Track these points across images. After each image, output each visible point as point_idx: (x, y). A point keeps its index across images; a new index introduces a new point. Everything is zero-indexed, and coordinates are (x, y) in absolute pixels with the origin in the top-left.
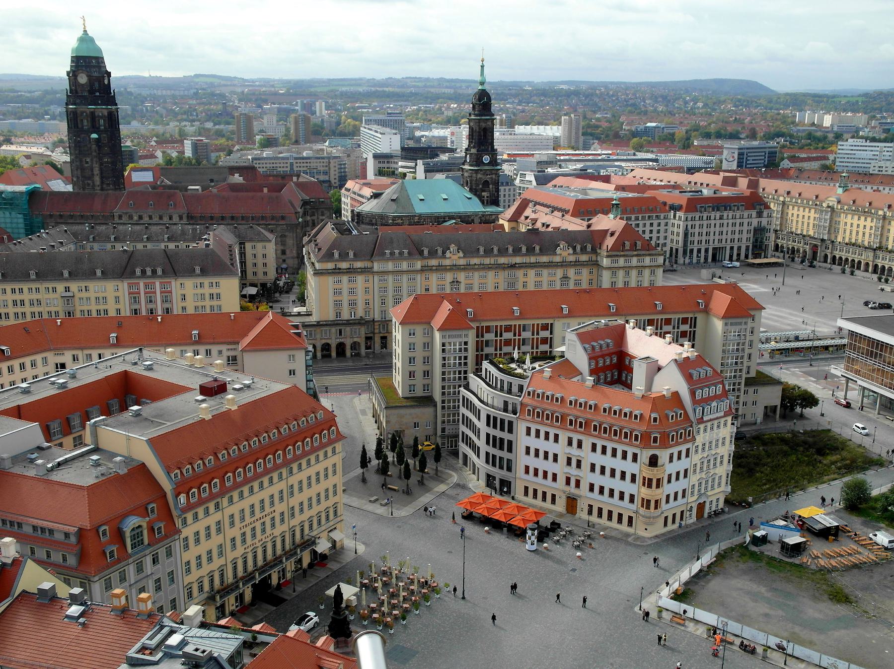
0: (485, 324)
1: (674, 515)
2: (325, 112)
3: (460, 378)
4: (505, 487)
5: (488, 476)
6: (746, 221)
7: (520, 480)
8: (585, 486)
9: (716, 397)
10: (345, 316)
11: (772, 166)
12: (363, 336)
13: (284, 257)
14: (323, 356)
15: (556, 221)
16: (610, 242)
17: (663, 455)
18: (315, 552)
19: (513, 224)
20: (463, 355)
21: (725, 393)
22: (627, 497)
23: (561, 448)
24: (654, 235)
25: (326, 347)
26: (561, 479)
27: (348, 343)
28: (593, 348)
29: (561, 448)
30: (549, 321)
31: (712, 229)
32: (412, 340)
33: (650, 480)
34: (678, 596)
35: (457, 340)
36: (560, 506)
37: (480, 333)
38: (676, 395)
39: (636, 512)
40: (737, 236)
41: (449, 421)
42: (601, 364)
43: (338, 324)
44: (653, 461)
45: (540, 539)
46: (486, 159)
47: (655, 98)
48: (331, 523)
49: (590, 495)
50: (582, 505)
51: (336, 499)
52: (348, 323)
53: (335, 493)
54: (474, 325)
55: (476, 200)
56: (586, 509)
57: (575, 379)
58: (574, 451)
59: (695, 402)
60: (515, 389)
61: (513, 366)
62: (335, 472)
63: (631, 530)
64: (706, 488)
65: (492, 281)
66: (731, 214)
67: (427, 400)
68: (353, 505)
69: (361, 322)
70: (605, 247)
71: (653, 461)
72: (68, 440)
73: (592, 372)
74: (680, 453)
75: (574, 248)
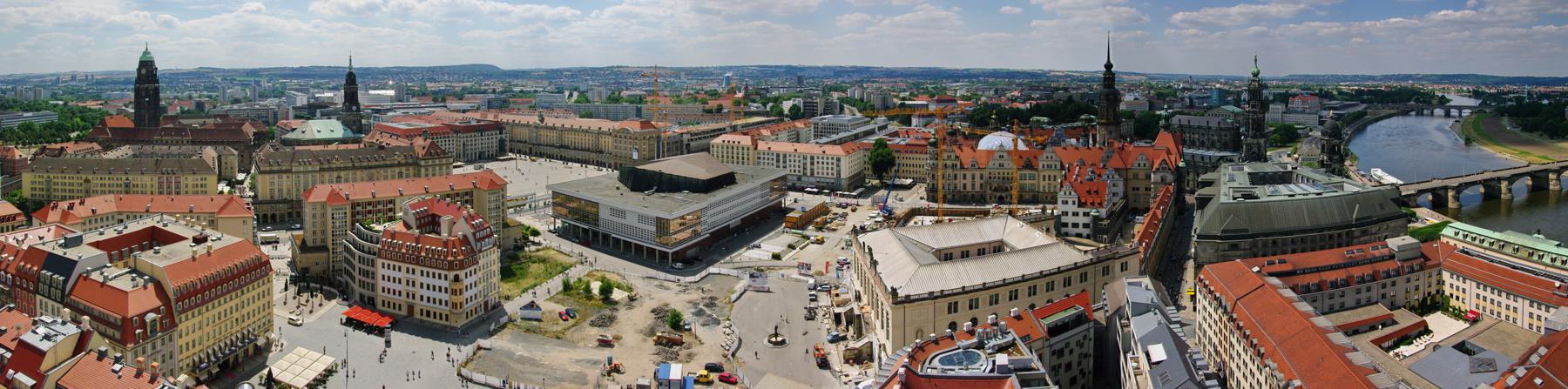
10: (276, 197)
17: (462, 274)
23: (402, 275)
25: (265, 216)
29: (402, 275)
43: (272, 202)
44: (457, 279)
50: (417, 310)
52: (279, 202)
58: (410, 276)
59: (477, 240)
67: (324, 248)
69: (285, 201)
71: (457, 279)
72: (121, 264)
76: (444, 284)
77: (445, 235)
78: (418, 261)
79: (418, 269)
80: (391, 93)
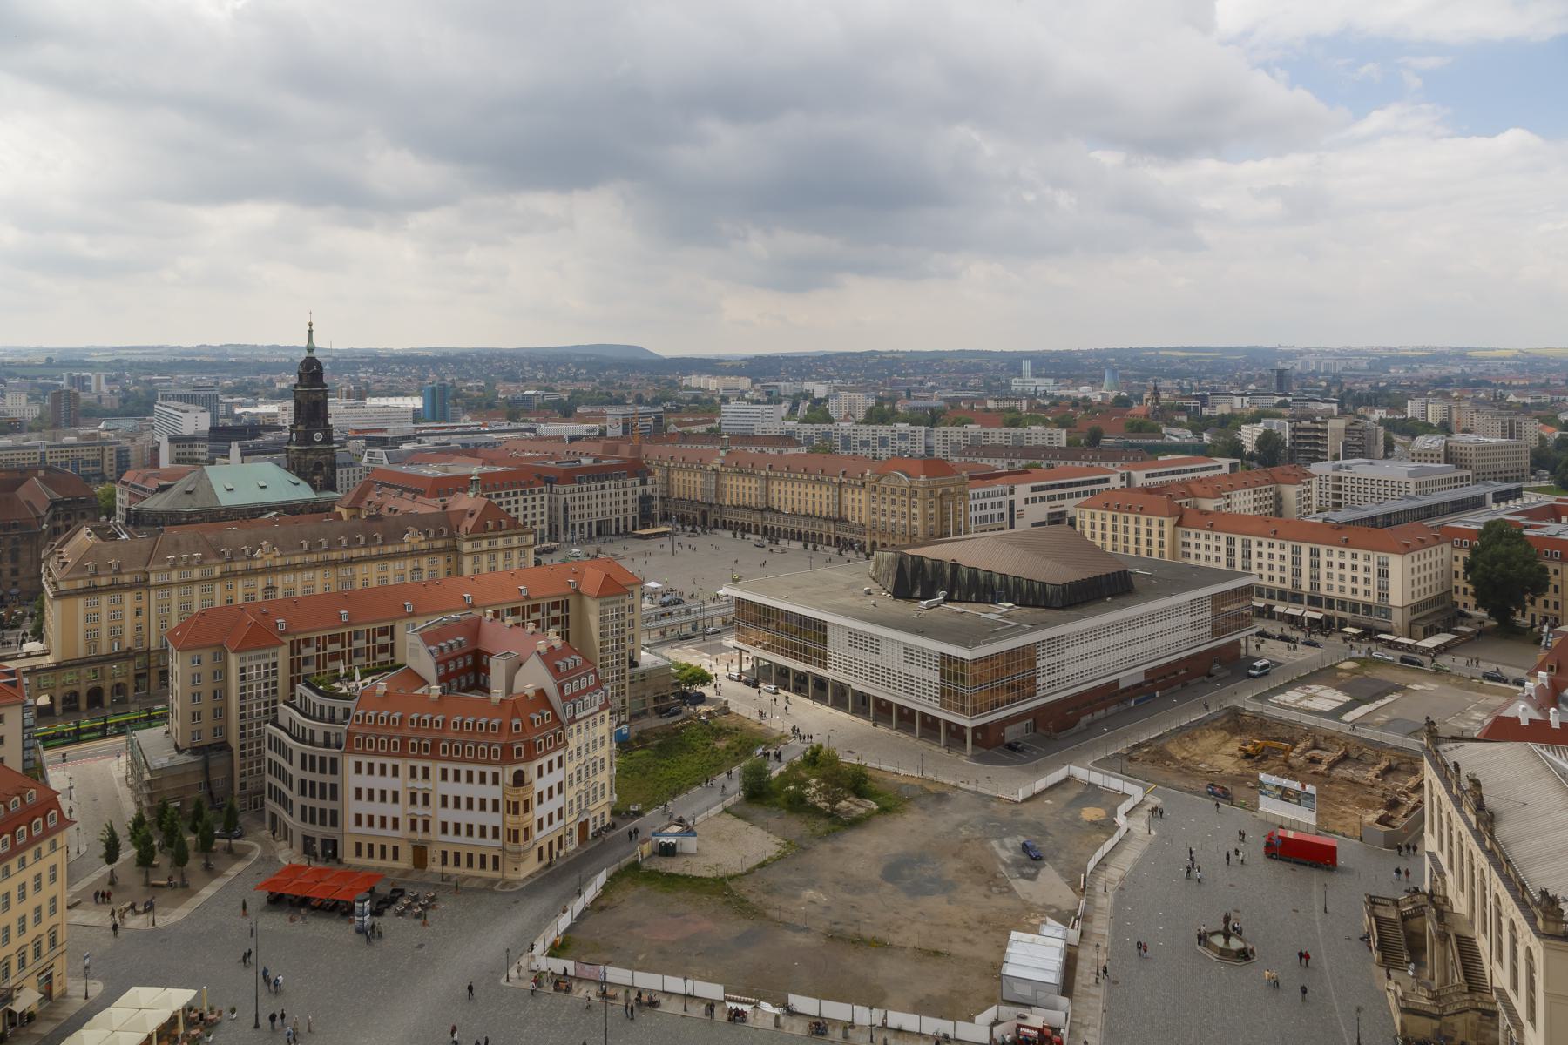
0: (301, 637)
1: (551, 844)
2: (105, 389)
3: (266, 712)
4: (331, 849)
5: (305, 838)
6: (630, 490)
7: (350, 833)
8: (435, 827)
9: (589, 689)
10: (104, 649)
11: (658, 431)
12: (132, 673)
13: (15, 579)
14: (65, 710)
15: (407, 505)
16: (469, 523)
17: (530, 770)
18: (11, 1013)
19: (353, 512)
20: (271, 680)
21: (599, 684)
22: (489, 832)
23: (402, 784)
24: (521, 513)
26: (404, 824)
27: (107, 685)
28: (441, 649)
29: (402, 784)
30: (389, 624)
31: (594, 501)
32: (197, 669)
33: (516, 804)
34: (556, 951)
35: (262, 662)
36: (405, 862)
37: (295, 648)
38: (541, 693)
39: (503, 849)
40: (621, 506)
41: (251, 772)
42: (452, 668)
43: (94, 661)
44: (519, 779)
45: (376, 913)
46: (318, 436)
47: (533, 365)
48: (45, 959)
49: (443, 838)
50: (434, 853)
51: (56, 919)
52: (109, 659)
53: (53, 910)
54: (287, 640)
55: (304, 485)
56: (439, 859)
57: (419, 692)
58: (419, 784)
59: (564, 698)
60: (339, 715)
61: (337, 685)
62: (53, 878)
63: (497, 875)
64: (587, 802)
65: (320, 581)
66: (613, 483)
68: (90, 922)
69: (128, 655)
70: (463, 530)
73: (441, 680)
74: (550, 763)
75: (427, 534)
76: (491, 792)
77: (498, 692)
78: (435, 751)
79: (435, 768)
80: (417, 402)
